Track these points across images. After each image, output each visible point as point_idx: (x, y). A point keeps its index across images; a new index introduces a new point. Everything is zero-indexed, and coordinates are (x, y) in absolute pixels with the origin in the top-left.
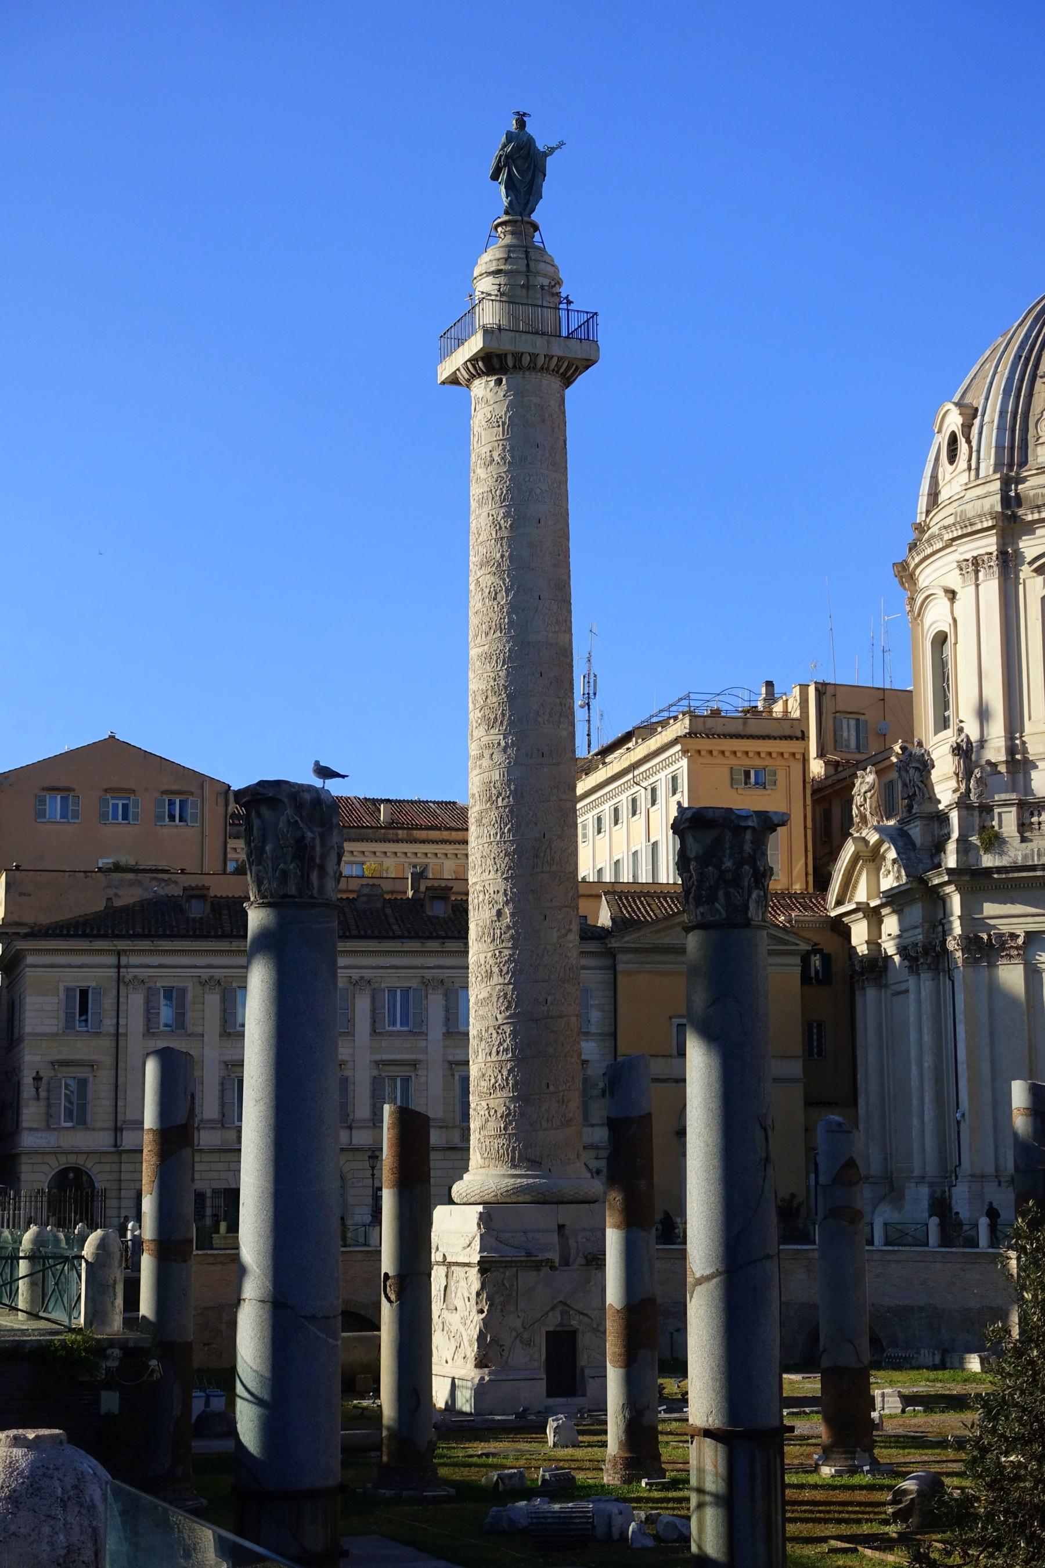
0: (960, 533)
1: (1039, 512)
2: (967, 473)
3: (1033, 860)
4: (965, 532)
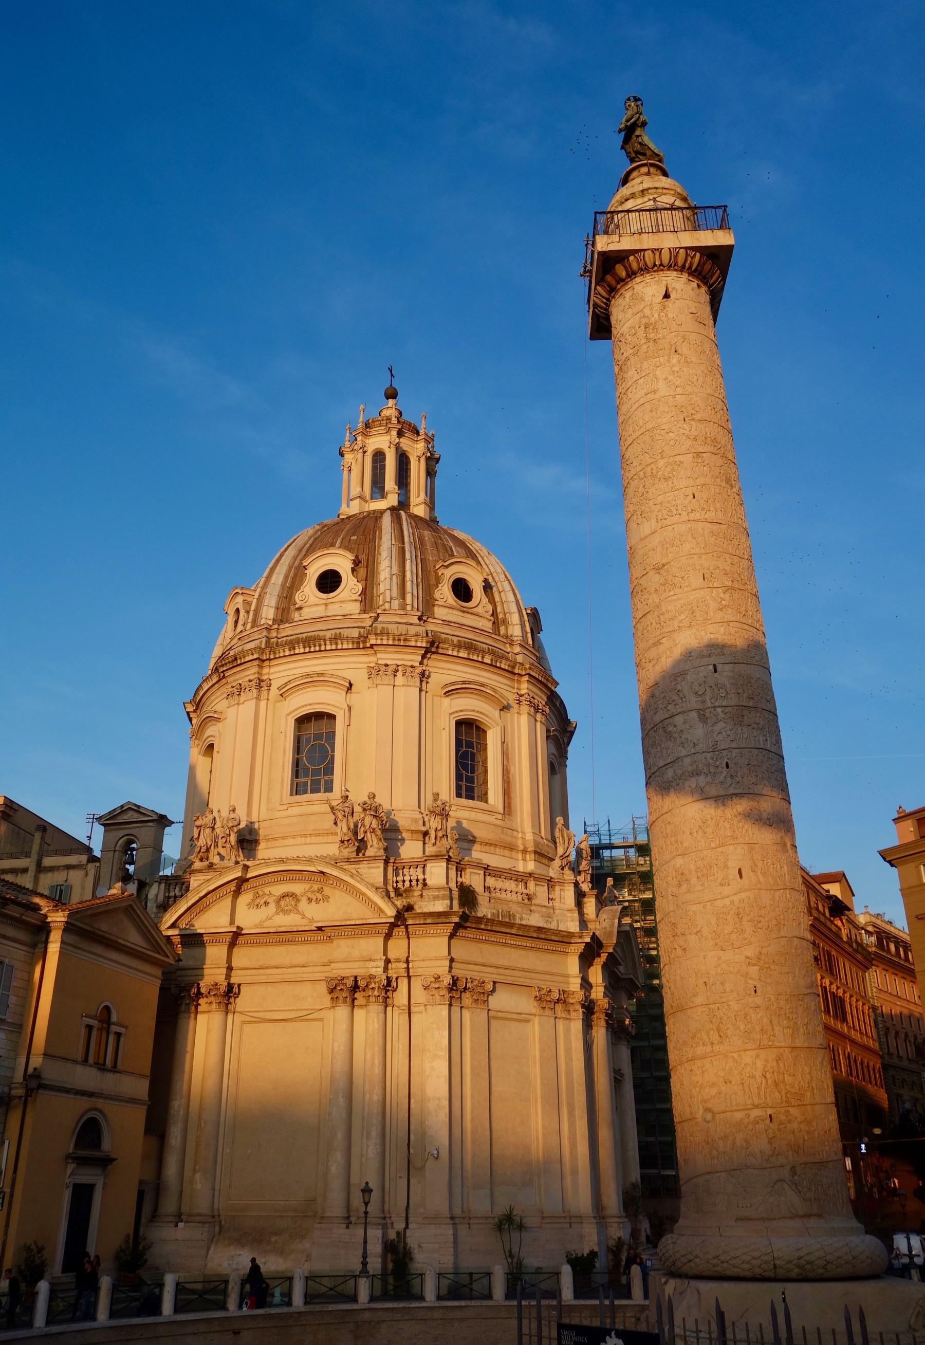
0: (391, 642)
1: (458, 651)
2: (358, 604)
3: (499, 917)
4: (396, 643)
